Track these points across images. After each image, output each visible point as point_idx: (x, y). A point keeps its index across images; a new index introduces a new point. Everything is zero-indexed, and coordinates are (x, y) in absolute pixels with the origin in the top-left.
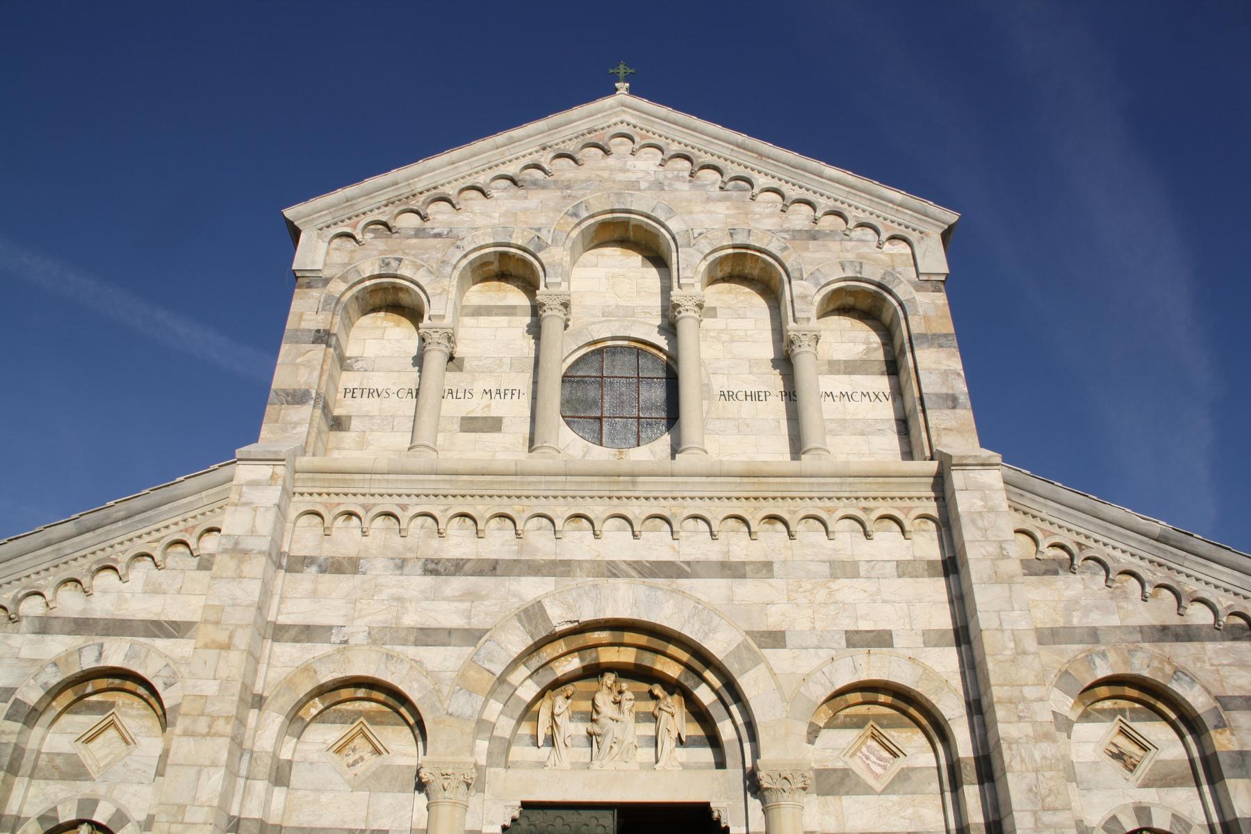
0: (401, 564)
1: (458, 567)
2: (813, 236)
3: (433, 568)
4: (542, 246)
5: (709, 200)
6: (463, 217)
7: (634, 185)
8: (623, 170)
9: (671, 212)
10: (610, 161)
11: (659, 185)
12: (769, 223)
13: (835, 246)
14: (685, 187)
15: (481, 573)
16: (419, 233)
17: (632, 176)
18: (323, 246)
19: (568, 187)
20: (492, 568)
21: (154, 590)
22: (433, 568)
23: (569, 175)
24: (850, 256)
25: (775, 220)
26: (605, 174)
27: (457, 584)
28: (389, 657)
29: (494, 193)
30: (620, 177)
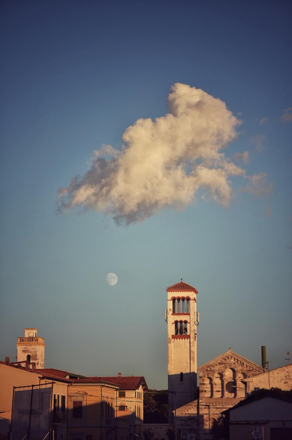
0: (214, 408)
1: (218, 408)
2: (250, 371)
3: (216, 408)
4: (223, 373)
5: (239, 366)
6: (214, 368)
7: (231, 363)
8: (231, 361)
9: (235, 368)
10: (229, 360)
11: (234, 364)
12: (245, 369)
13: (252, 372)
14: (237, 364)
15: (220, 408)
16: (211, 371)
17: (231, 362)
18: (201, 373)
19: (225, 364)
20: (221, 408)
21: (194, 411)
22: (216, 408)
23: (225, 362)
24: (253, 373)
25: (246, 369)
26: (229, 362)
27: (218, 410)
28: (214, 416)
29: (217, 365)
30: (230, 362)
